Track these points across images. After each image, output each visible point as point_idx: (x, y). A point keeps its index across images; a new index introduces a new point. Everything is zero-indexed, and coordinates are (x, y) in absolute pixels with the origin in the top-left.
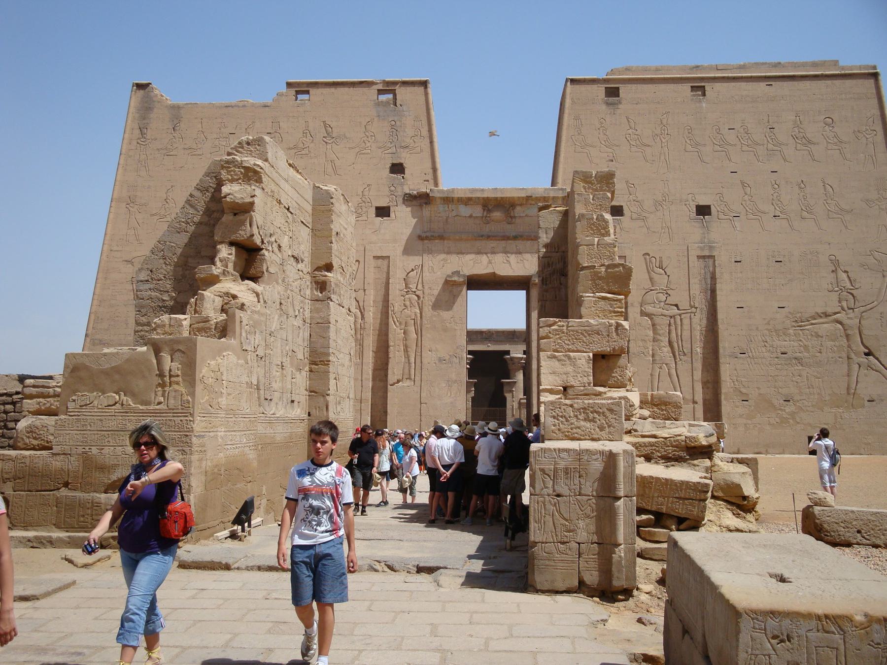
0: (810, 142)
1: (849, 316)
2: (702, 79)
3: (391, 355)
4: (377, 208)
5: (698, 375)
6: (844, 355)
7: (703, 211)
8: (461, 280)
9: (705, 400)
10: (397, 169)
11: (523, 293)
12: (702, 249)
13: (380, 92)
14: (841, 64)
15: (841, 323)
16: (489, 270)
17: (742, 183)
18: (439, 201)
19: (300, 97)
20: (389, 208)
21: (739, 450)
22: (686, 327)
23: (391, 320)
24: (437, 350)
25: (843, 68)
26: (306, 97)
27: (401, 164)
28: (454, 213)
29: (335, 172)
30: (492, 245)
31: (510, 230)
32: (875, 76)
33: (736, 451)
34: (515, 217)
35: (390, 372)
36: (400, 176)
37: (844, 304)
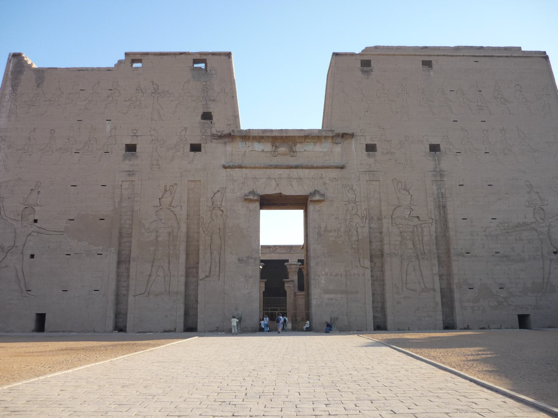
0: (506, 100)
1: (541, 225)
2: (430, 55)
5: (436, 269)
6: (539, 253)
7: (434, 148)
8: (256, 198)
9: (441, 289)
10: (207, 116)
12: (435, 176)
13: (196, 61)
14: (523, 49)
19: (135, 65)
21: (468, 326)
23: (201, 229)
25: (524, 52)
26: (139, 65)
27: (211, 113)
28: (250, 149)
30: (279, 172)
31: (293, 161)
32: (546, 58)
33: (466, 326)
34: (296, 152)
36: (208, 122)
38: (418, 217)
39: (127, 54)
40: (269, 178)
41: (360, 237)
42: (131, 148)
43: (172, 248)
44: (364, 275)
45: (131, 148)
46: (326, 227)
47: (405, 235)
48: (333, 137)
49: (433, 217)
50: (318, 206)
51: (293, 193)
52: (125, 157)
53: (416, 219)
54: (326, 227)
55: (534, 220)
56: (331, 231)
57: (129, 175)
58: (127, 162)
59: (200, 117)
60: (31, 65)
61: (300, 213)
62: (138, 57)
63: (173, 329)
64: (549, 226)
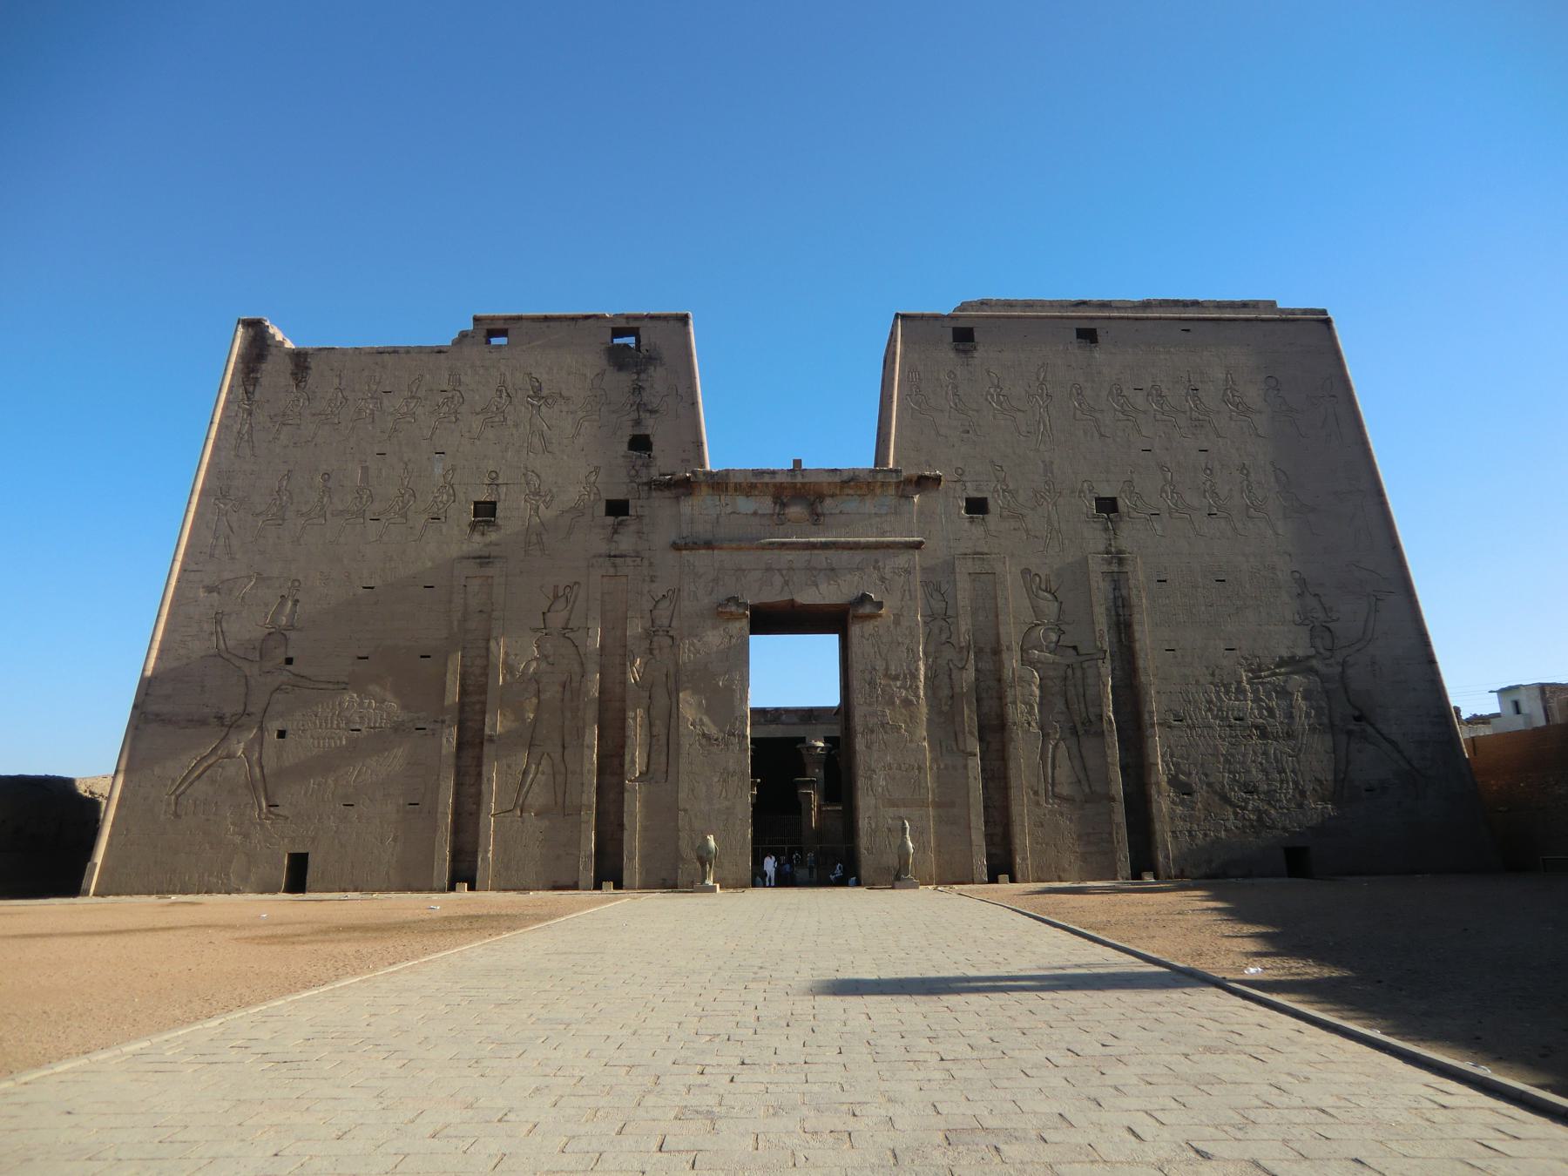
2: (1092, 318)
3: (630, 733)
4: (609, 503)
5: (1114, 754)
7: (1107, 506)
10: (640, 443)
11: (833, 640)
12: (1110, 563)
13: (618, 332)
15: (1316, 673)
16: (786, 597)
17: (1162, 467)
18: (705, 490)
19: (494, 341)
20: (627, 502)
22: (1090, 681)
24: (702, 723)
25: (1283, 311)
26: (503, 341)
27: (647, 437)
28: (729, 509)
29: (545, 450)
32: (1328, 322)
35: (628, 758)
37: (1318, 642)
38: (1075, 648)
39: (476, 319)
40: (769, 569)
41: (957, 690)
42: (486, 511)
43: (568, 715)
44: (965, 767)
45: (486, 511)
46: (887, 669)
47: (1050, 683)
48: (898, 484)
49: (1106, 647)
50: (869, 627)
51: (818, 600)
52: (473, 526)
53: (1072, 652)
54: (887, 669)
55: (1312, 652)
56: (896, 678)
57: (481, 565)
58: (477, 537)
59: (625, 446)
60: (282, 343)
61: (829, 643)
62: (499, 325)
63: (571, 883)
64: (1344, 664)
